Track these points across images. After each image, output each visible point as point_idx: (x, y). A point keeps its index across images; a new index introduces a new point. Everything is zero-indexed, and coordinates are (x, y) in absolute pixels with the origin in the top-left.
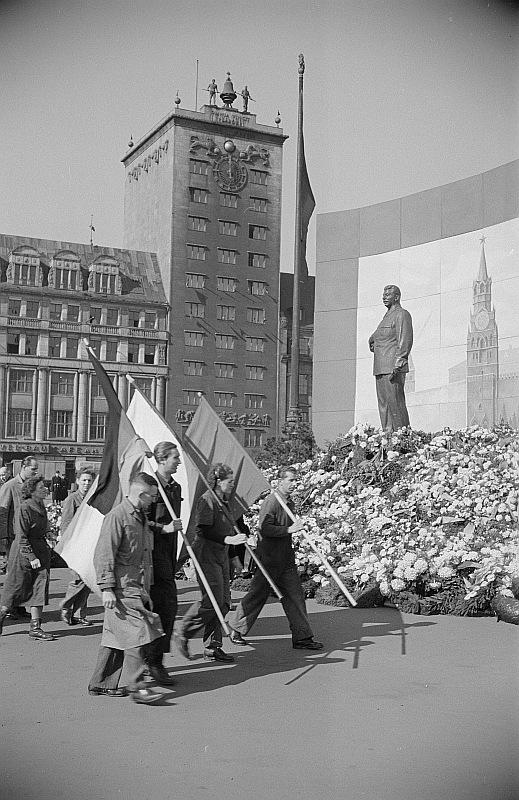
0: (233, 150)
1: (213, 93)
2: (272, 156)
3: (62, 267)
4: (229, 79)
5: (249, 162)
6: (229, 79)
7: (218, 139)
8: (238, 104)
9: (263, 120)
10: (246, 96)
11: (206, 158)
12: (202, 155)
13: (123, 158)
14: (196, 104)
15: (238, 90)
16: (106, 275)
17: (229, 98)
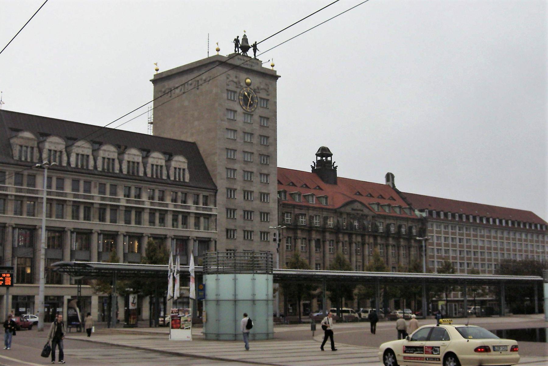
1: (236, 46)
2: (270, 88)
3: (155, 163)
4: (245, 35)
5: (259, 92)
6: (245, 35)
8: (250, 53)
9: (266, 65)
10: (255, 46)
11: (235, 89)
12: (232, 87)
13: (152, 78)
14: (228, 50)
15: (251, 43)
16: (180, 169)
17: (245, 48)
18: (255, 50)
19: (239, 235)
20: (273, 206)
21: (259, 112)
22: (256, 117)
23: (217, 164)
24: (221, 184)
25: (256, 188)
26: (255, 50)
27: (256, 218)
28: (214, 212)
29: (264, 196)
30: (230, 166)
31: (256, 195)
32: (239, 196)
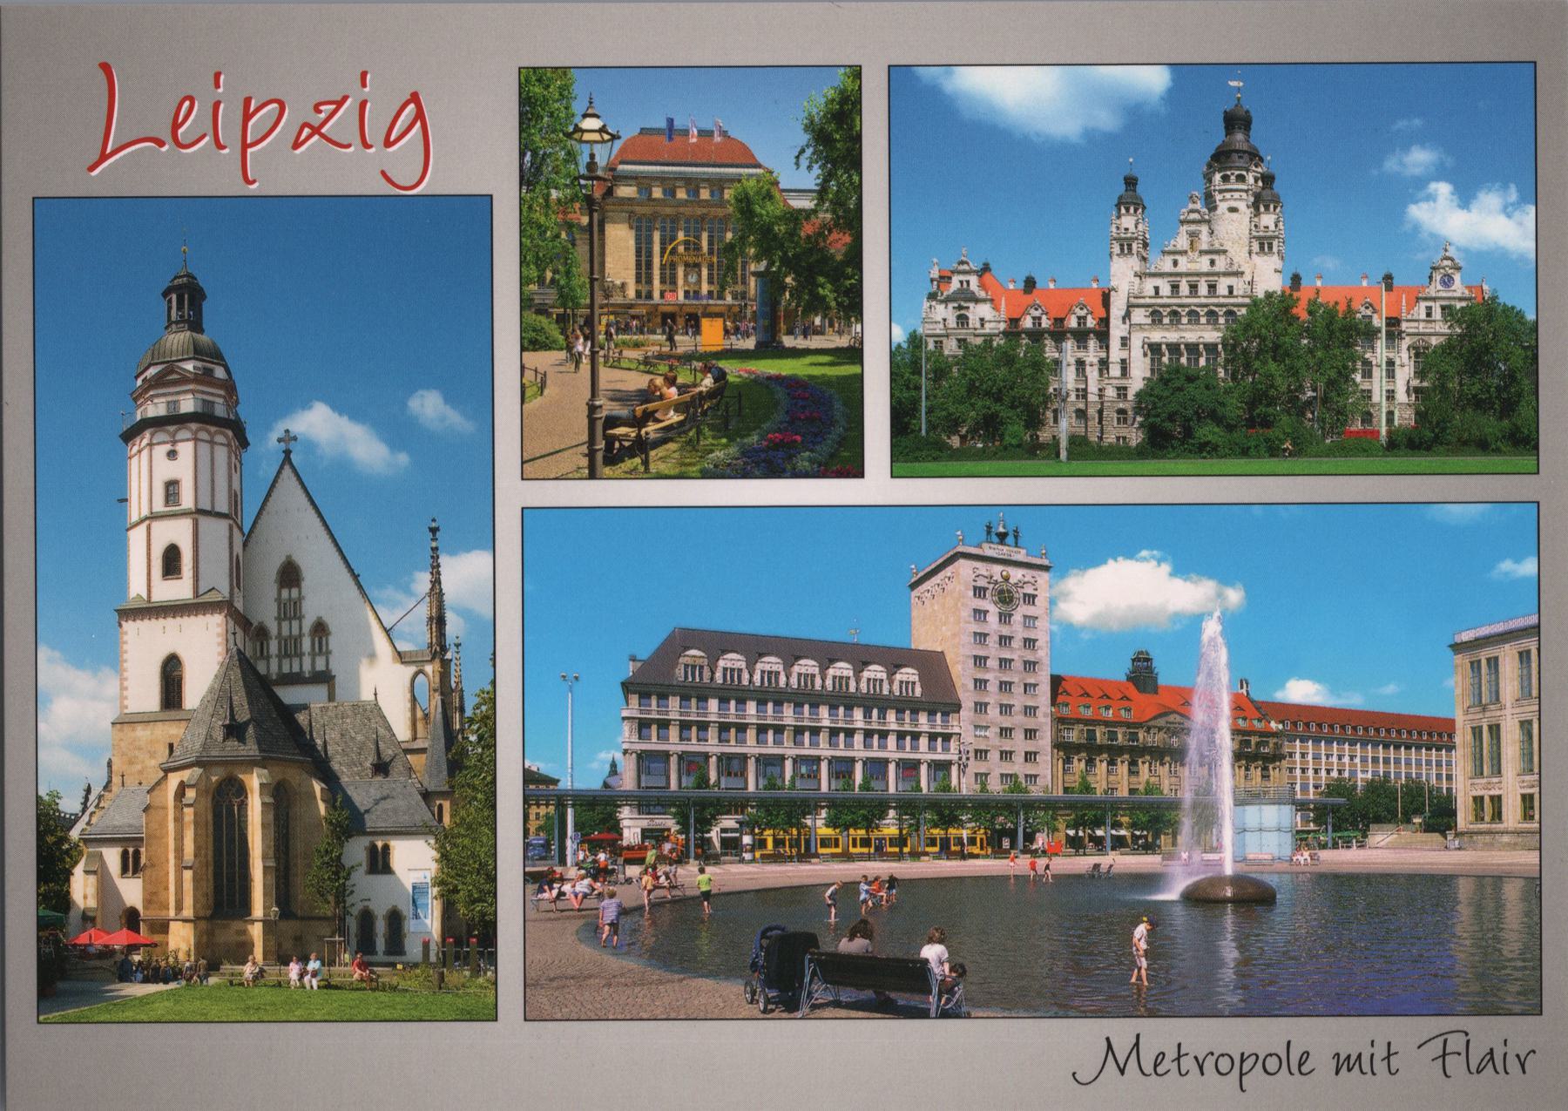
0: (1007, 579)
1: (989, 533)
7: (997, 569)
10: (1016, 531)
12: (982, 583)
18: (1016, 537)
19: (994, 756)
20: (1043, 720)
21: (1022, 610)
22: (1017, 617)
23: (962, 674)
24: (967, 697)
25: (1018, 700)
26: (1016, 537)
27: (1019, 735)
28: (956, 730)
29: (1030, 711)
30: (979, 676)
31: (1018, 708)
32: (993, 712)
